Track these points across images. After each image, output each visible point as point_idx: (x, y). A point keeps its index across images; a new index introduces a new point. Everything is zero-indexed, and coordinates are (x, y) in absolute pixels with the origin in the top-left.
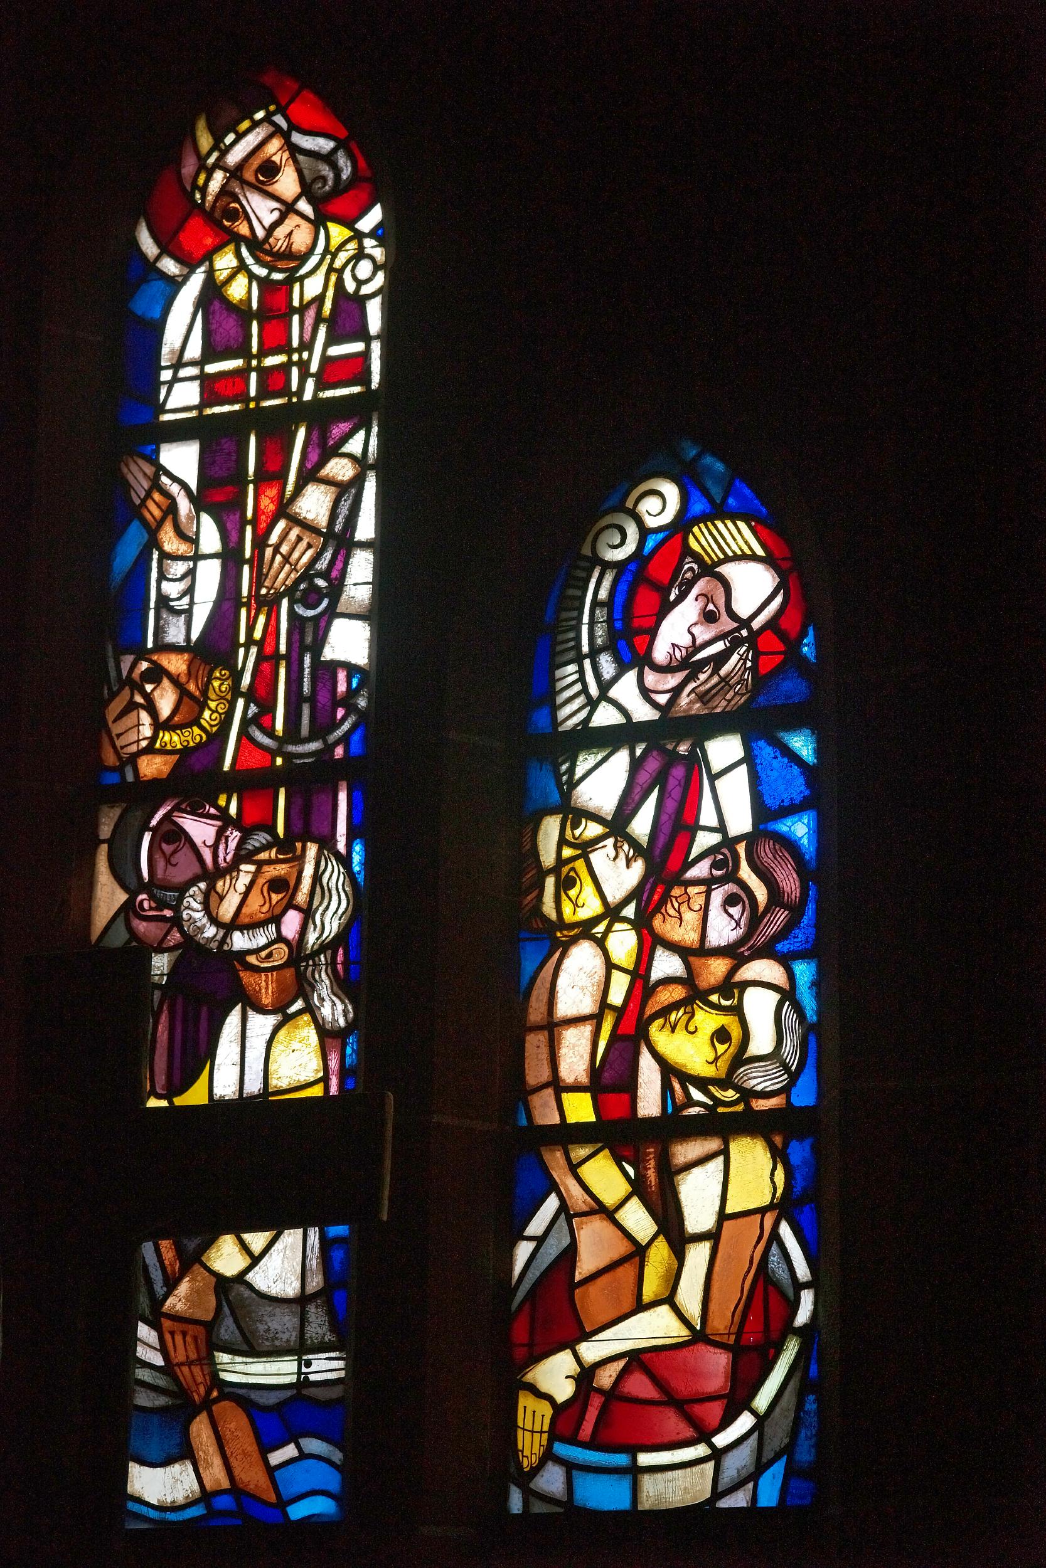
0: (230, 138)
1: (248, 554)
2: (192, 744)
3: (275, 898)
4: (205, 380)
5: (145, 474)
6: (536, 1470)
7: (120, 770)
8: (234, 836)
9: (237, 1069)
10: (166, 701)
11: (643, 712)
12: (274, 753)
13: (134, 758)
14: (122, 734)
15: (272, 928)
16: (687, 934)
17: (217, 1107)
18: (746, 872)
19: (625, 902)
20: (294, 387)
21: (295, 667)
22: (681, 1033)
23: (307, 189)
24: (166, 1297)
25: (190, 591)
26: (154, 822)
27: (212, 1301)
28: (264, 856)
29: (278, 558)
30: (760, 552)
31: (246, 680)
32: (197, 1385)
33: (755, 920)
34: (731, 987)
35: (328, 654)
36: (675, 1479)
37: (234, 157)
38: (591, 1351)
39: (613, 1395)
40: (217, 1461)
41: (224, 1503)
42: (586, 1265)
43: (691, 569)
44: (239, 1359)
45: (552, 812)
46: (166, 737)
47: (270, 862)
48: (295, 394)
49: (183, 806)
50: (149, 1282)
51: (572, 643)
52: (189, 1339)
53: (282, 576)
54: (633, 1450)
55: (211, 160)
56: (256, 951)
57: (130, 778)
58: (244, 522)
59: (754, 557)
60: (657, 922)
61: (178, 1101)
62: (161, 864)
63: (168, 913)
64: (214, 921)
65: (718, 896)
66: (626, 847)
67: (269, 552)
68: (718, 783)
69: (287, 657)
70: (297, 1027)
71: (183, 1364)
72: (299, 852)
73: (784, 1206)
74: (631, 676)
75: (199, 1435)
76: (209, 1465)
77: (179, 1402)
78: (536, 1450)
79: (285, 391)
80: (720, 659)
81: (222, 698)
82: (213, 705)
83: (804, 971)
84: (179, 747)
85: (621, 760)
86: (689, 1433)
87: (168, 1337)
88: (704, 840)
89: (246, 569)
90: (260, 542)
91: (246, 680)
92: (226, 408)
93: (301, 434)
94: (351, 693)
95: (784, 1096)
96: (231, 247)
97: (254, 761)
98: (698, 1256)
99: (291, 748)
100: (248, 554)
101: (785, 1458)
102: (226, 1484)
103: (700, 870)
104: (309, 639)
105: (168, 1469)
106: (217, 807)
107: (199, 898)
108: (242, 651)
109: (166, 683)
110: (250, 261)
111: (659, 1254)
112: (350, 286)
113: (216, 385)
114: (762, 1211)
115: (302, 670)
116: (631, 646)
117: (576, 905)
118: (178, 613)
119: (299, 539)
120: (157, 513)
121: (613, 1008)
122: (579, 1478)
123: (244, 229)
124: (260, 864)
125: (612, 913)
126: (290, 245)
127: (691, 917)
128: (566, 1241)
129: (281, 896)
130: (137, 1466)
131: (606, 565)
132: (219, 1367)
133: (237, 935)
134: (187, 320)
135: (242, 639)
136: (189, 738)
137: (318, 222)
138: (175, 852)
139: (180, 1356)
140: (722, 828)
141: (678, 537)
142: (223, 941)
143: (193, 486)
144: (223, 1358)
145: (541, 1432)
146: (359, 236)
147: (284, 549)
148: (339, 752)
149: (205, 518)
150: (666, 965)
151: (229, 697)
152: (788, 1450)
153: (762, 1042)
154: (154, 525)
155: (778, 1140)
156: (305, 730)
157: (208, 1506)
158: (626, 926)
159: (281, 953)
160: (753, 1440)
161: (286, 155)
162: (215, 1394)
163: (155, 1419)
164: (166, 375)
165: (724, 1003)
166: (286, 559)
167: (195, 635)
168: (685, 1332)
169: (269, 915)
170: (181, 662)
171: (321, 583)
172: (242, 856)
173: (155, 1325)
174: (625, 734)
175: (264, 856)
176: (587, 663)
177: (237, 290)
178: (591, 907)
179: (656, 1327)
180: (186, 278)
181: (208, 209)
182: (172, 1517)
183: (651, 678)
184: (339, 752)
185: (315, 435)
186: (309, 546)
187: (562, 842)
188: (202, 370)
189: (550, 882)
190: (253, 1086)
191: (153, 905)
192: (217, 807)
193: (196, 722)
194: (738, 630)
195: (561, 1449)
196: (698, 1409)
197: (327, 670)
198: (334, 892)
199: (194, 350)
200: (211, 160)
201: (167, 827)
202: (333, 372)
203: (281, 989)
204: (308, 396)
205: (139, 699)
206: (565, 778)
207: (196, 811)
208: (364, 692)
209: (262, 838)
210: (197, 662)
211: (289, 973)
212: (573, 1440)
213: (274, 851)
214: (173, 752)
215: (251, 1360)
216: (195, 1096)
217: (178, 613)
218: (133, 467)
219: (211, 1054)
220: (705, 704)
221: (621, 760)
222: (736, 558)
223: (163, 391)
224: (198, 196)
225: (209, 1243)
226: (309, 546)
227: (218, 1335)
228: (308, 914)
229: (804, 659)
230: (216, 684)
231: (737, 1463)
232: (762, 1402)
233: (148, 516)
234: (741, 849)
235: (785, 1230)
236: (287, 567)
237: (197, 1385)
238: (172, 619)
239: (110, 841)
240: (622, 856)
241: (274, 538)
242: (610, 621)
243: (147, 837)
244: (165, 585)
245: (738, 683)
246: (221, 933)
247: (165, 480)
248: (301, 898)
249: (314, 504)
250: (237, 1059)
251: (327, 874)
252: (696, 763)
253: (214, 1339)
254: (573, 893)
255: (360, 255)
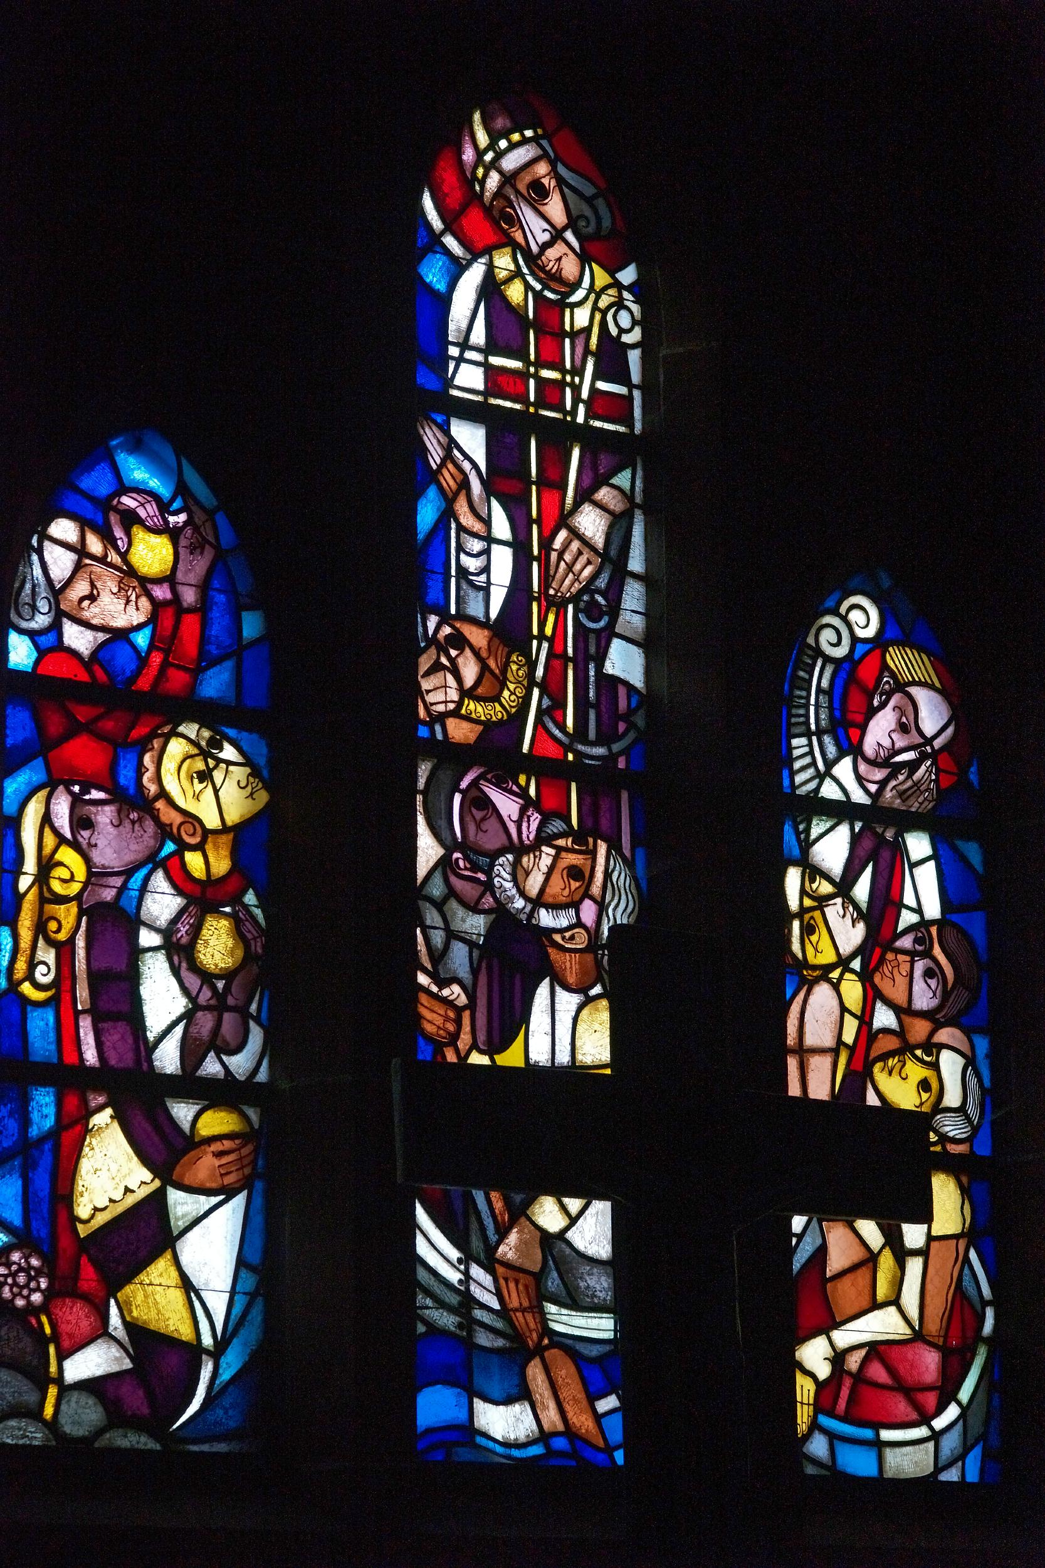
0: (503, 144)
1: (536, 552)
2: (494, 719)
3: (575, 885)
4: (490, 372)
5: (439, 441)
6: (807, 1437)
7: (430, 725)
8: (535, 819)
9: (549, 1038)
10: (470, 672)
11: (859, 796)
12: (568, 748)
13: (442, 717)
14: (430, 691)
15: (572, 912)
16: (900, 998)
17: (531, 1069)
18: (937, 951)
19: (853, 956)
20: (568, 406)
21: (581, 675)
22: (895, 1077)
23: (572, 223)
24: (499, 1242)
25: (486, 569)
26: (464, 784)
27: (538, 1255)
28: (561, 842)
29: (562, 564)
30: (938, 684)
31: (540, 672)
32: (530, 1331)
33: (946, 995)
34: (932, 1047)
35: (609, 669)
36: (908, 1452)
37: (510, 162)
38: (843, 1337)
39: (860, 1378)
40: (552, 1405)
41: (560, 1443)
42: (836, 1262)
43: (888, 682)
44: (564, 1311)
45: (796, 863)
46: (471, 706)
47: (567, 850)
48: (569, 413)
49: (489, 776)
50: (483, 1229)
51: (802, 719)
52: (521, 1287)
53: (567, 582)
54: (877, 1426)
55: (489, 157)
56: (561, 931)
57: (439, 736)
58: (530, 521)
59: (930, 686)
60: (877, 979)
61: (502, 1060)
62: (472, 828)
63: (482, 877)
64: (522, 893)
65: (920, 966)
66: (851, 908)
67: (554, 556)
68: (917, 871)
69: (574, 660)
70: (597, 1010)
71: (516, 1310)
72: (591, 846)
73: (971, 1235)
74: (847, 761)
75: (535, 1379)
76: (546, 1408)
77: (515, 1346)
78: (805, 1420)
79: (559, 407)
80: (913, 766)
81: (519, 682)
82: (512, 686)
83: (982, 1045)
84: (483, 718)
85: (843, 833)
86: (914, 1416)
87: (502, 1282)
88: (907, 918)
89: (535, 565)
90: (546, 544)
91: (540, 672)
92: (508, 404)
93: (576, 453)
94: (631, 711)
95: (968, 1144)
96: (508, 250)
97: (551, 750)
98: (914, 1266)
99: (580, 747)
100: (536, 552)
101: (981, 1443)
102: (561, 1427)
103: (906, 942)
104: (592, 650)
105: (510, 1407)
106: (519, 786)
107: (508, 869)
108: (535, 642)
109: (468, 652)
110: (525, 270)
111: (887, 1261)
112: (614, 331)
113: (500, 379)
114: (955, 1237)
115: (587, 677)
116: (847, 736)
117: (816, 950)
118: (478, 588)
119: (580, 553)
120: (451, 482)
121: (846, 1045)
122: (840, 1448)
123: (518, 237)
124: (559, 850)
125: (843, 962)
126: (560, 270)
127: (901, 982)
128: (819, 1241)
129: (578, 884)
130: (482, 1403)
131: (828, 659)
132: (548, 1316)
133: (543, 911)
134: (472, 306)
135: (535, 631)
136: (492, 712)
137: (584, 258)
138: (483, 819)
139: (514, 1303)
140: (919, 910)
141: (878, 652)
142: (531, 915)
143: (483, 467)
144: (551, 1308)
145: (809, 1404)
146: (617, 284)
147: (568, 557)
148: (622, 764)
149: (495, 505)
150: (884, 1018)
151: (525, 683)
152: (982, 1438)
153: (952, 1098)
154: (450, 495)
155: (964, 1180)
156: (592, 734)
157: (547, 1446)
158: (853, 977)
159: (581, 940)
160: (959, 1426)
161: (553, 183)
162: (546, 1341)
163: (495, 1359)
164: (454, 351)
165: (927, 1059)
166: (570, 567)
167: (493, 614)
168: (908, 1331)
169: (569, 900)
170: (481, 636)
171: (600, 599)
172: (543, 839)
173: (489, 1269)
174: (841, 811)
175: (561, 842)
176: (814, 739)
177: (515, 292)
178: (827, 956)
179: (883, 1325)
180: (469, 264)
181: (488, 204)
182: (516, 1453)
183: (863, 767)
184: (622, 764)
185: (587, 462)
186: (589, 563)
187: (803, 892)
188: (486, 359)
189: (796, 924)
190: (563, 1058)
191: (468, 866)
192: (519, 786)
193: (496, 698)
194: (924, 745)
195: (823, 1420)
196: (920, 1397)
197: (611, 683)
198: (623, 891)
199: (479, 336)
200: (489, 157)
201: (474, 793)
202: (598, 403)
203: (583, 971)
204: (580, 419)
205: (444, 660)
206: (802, 836)
207: (499, 784)
208: (641, 712)
209: (557, 826)
210: (496, 641)
211: (589, 958)
212: (831, 1414)
213: (570, 840)
214: (477, 722)
215: (574, 1313)
216: (511, 1058)
217: (478, 588)
218: (427, 430)
219: (524, 1017)
220: (903, 801)
221: (843, 833)
222: (920, 684)
223: (452, 366)
224: (477, 188)
225: (531, 1201)
226: (589, 563)
227: (546, 1289)
228: (602, 907)
229: (970, 784)
230: (514, 667)
231: (951, 1443)
232: (964, 1395)
233: (445, 484)
234: (934, 930)
235: (973, 1255)
236: (571, 576)
237: (530, 1331)
238: (472, 593)
239: (424, 793)
240: (848, 915)
241: (558, 544)
242: (831, 708)
243: (458, 798)
244: (463, 556)
245: (926, 790)
246: (529, 907)
247: (456, 452)
248: (596, 889)
249: (591, 523)
250: (549, 1029)
251: (616, 874)
252: (899, 850)
253: (543, 1290)
254: (814, 938)
255: (619, 305)
